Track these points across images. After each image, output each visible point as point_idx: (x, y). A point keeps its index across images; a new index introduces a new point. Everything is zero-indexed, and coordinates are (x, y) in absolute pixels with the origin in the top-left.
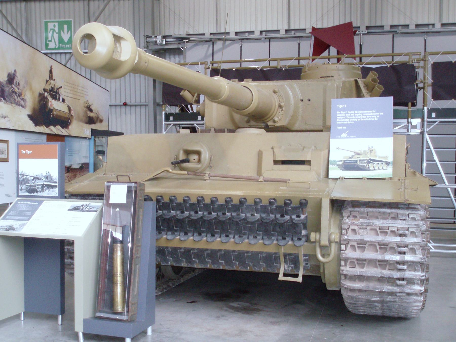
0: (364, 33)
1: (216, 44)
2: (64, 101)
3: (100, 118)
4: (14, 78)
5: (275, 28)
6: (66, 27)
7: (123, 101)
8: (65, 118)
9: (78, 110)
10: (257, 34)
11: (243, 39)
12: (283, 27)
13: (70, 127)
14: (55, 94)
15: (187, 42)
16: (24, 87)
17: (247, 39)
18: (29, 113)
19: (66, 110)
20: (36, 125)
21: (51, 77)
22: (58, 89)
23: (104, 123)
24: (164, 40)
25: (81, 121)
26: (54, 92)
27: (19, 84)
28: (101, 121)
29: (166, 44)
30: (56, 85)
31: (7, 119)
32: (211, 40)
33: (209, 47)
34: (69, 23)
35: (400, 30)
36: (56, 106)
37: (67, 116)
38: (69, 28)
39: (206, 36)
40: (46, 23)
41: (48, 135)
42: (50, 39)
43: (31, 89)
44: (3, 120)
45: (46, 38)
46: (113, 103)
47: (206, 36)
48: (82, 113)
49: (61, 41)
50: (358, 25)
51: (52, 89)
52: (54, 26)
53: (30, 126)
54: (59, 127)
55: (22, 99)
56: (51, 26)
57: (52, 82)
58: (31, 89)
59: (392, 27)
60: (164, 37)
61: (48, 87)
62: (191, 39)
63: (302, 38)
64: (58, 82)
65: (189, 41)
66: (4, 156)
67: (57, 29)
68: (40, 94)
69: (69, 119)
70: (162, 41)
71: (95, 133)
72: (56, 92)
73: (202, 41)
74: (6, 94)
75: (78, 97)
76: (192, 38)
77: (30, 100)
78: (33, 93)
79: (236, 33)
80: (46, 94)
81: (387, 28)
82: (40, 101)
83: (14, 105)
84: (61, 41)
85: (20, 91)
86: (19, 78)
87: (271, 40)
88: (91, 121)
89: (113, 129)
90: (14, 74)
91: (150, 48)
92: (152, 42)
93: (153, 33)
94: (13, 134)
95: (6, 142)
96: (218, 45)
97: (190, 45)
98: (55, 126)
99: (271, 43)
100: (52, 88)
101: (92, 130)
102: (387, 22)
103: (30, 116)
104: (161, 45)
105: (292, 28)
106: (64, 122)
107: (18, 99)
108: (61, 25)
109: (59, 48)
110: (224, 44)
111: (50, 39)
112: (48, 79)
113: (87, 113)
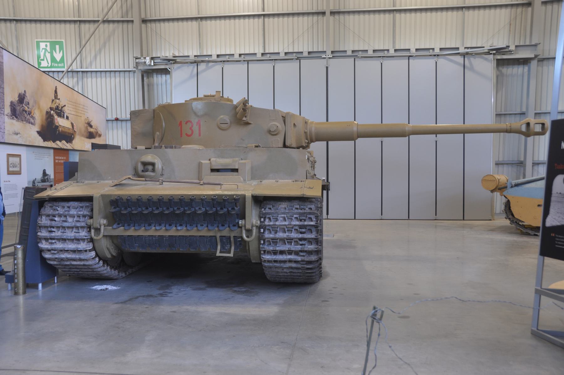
0: (330, 56)
2: (67, 118)
3: (99, 132)
4: (24, 98)
5: (252, 52)
6: (57, 47)
7: (114, 117)
8: (69, 133)
9: (80, 126)
10: (237, 57)
11: (224, 61)
12: (259, 51)
13: (74, 142)
14: (60, 112)
15: (174, 63)
16: (33, 106)
17: (228, 61)
18: (38, 130)
19: (70, 127)
20: (45, 140)
21: (56, 97)
22: (62, 107)
23: (102, 138)
24: (152, 61)
25: (83, 136)
26: (59, 110)
27: (28, 104)
28: (100, 136)
29: (154, 65)
30: (61, 103)
31: (19, 135)
32: (195, 62)
33: (194, 67)
34: (60, 44)
35: (360, 54)
36: (61, 122)
37: (71, 131)
38: (61, 49)
39: (190, 58)
40: (38, 43)
41: (54, 149)
42: (42, 58)
43: (39, 108)
44: (15, 137)
45: (39, 57)
46: (109, 117)
47: (190, 58)
48: (83, 129)
49: (53, 59)
50: (325, 50)
51: (57, 108)
52: (46, 46)
53: (39, 141)
54: (64, 142)
55: (32, 117)
56: (42, 45)
57: (57, 101)
58: (39, 108)
59: (353, 51)
60: (152, 58)
61: (54, 106)
62: (178, 60)
64: (63, 101)
65: (175, 62)
66: (17, 169)
67: (48, 49)
68: (47, 112)
69: (73, 134)
70: (151, 62)
71: (94, 146)
72: (61, 110)
73: (187, 63)
74: (18, 112)
75: (79, 115)
76: (178, 60)
77: (39, 117)
78: (41, 111)
79: (218, 56)
80: (52, 112)
81: (349, 53)
82: (47, 119)
83: (25, 122)
84: (53, 59)
85: (29, 110)
86: (28, 98)
88: (91, 136)
89: (110, 142)
90: (24, 95)
91: (139, 68)
92: (141, 63)
93: (142, 55)
94: (24, 148)
95: (19, 156)
96: (202, 67)
97: (176, 66)
98: (60, 141)
100: (58, 106)
101: (92, 144)
102: (349, 47)
103: (38, 132)
104: (150, 65)
105: (267, 51)
106: (69, 138)
107: (28, 117)
108: (53, 45)
109: (51, 67)
110: (207, 65)
111: (42, 58)
112: (54, 98)
113: (87, 129)
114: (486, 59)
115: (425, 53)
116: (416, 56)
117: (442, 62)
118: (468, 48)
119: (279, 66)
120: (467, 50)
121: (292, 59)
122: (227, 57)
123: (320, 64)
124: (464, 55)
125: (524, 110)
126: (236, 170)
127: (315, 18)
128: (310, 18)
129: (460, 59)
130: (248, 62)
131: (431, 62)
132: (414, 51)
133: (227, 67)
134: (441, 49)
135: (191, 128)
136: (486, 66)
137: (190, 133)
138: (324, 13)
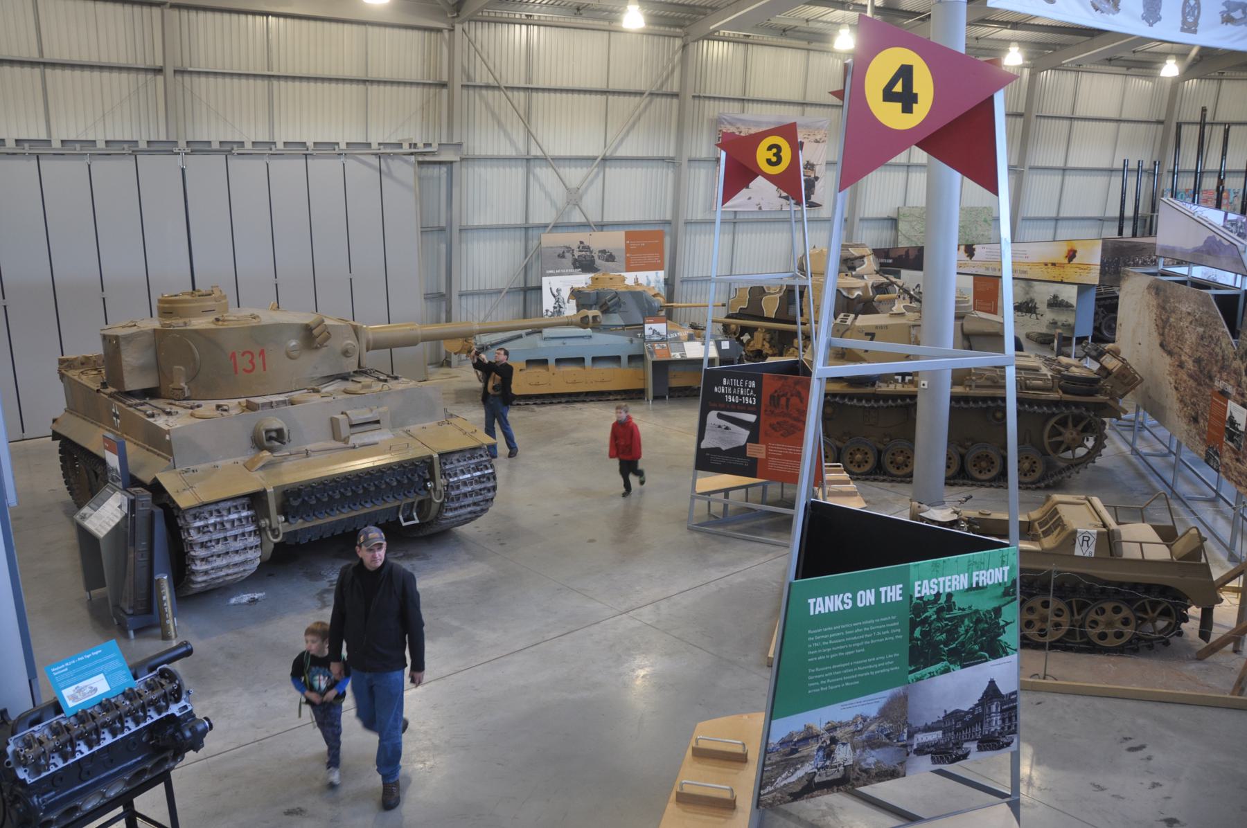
81: (216, 146)
114: (406, 162)
115: (327, 149)
117: (351, 164)
119: (99, 166)
125: (443, 224)
126: (378, 422)
127: (141, 76)
128: (133, 75)
131: (338, 163)
135: (251, 362)
136: (404, 170)
137: (249, 367)
138: (158, 71)
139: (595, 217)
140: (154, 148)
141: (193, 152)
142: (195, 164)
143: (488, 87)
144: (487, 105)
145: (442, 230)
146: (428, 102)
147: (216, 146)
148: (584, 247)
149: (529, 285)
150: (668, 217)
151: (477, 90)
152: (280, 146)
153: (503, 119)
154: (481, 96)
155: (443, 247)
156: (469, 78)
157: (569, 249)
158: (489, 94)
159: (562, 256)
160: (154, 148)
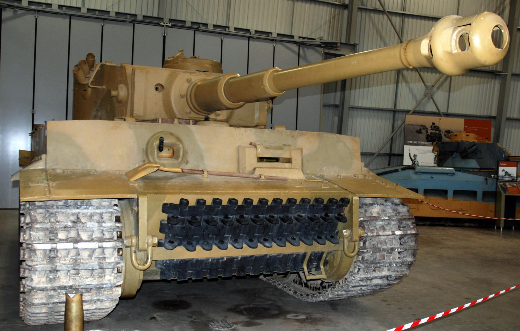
0: (168, 25)
1: (5, 11)
11: (39, 11)
17: (44, 11)
35: (202, 28)
63: (106, 21)
87: (72, 17)
99: (72, 20)
114: (317, 51)
115: (264, 36)
116: (257, 38)
118: (304, 38)
119: (109, 27)
120: (301, 40)
121: (125, 22)
122: (44, 6)
123: (156, 32)
124: (299, 44)
125: (337, 103)
129: (295, 48)
130: (70, 17)
131: (269, 46)
132: (254, 33)
133: (43, 19)
134: (278, 35)
139: (443, 110)
140: (148, 20)
141: (173, 26)
142: (173, 34)
143: (375, 11)
144: (374, 23)
145: (336, 106)
146: (334, 17)
147: (188, 24)
148: (434, 127)
149: (393, 152)
150: (494, 114)
151: (368, 13)
152: (232, 30)
153: (384, 34)
154: (370, 18)
155: (336, 119)
156: (362, 4)
157: (424, 127)
158: (375, 17)
159: (419, 132)
160: (148, 20)
